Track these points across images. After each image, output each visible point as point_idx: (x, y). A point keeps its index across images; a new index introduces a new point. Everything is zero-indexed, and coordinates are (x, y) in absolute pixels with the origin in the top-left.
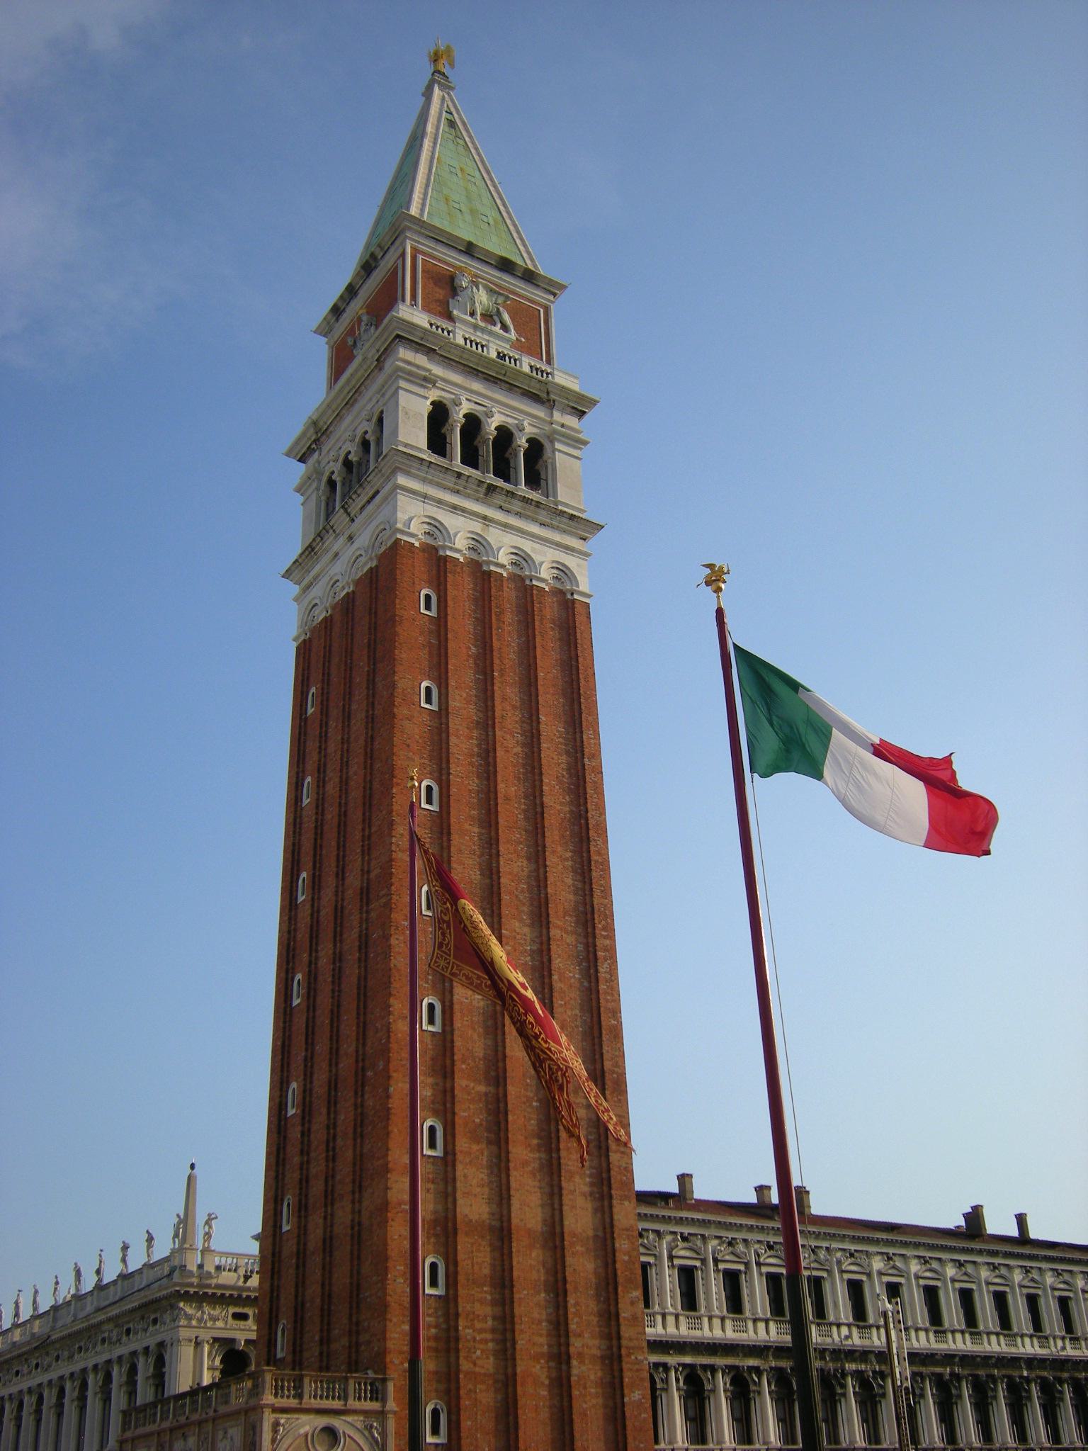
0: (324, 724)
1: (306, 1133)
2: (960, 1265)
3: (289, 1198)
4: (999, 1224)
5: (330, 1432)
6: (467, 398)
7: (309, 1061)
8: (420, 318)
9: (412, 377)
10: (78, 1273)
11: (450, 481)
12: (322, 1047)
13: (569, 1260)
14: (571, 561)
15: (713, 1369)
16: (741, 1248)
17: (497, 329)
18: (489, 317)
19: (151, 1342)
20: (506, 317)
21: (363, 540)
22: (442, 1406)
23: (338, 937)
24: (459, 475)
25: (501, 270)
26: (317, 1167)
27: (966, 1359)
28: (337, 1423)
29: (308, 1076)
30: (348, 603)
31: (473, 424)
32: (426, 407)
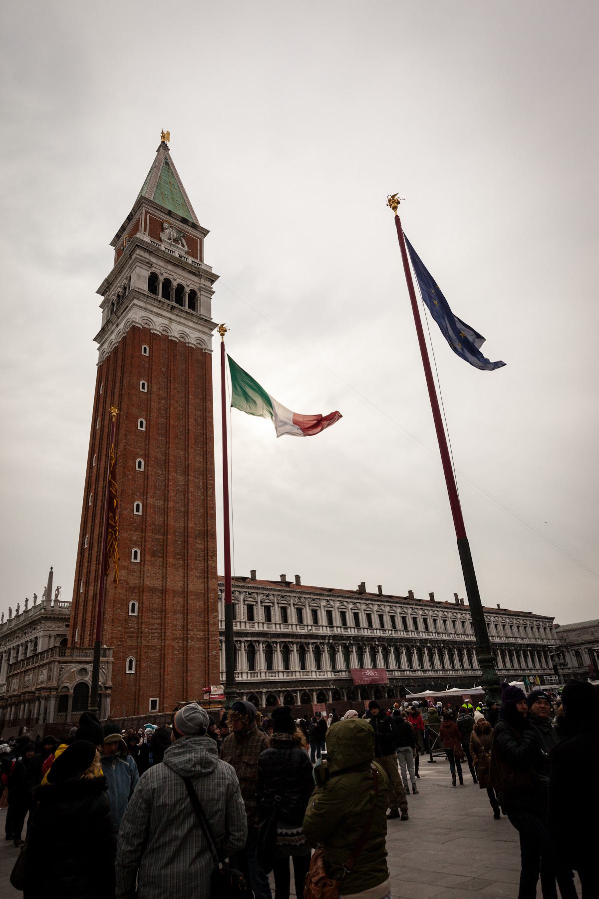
0: (105, 397)
1: (90, 554)
2: (354, 604)
4: (371, 589)
5: (85, 670)
6: (165, 272)
7: (93, 527)
8: (147, 239)
9: (142, 262)
10: (10, 610)
11: (156, 304)
15: (259, 642)
16: (272, 597)
17: (180, 246)
19: (32, 637)
20: (184, 241)
22: (134, 659)
24: (160, 301)
27: (355, 638)
29: (92, 532)
30: (115, 351)
31: (167, 282)
32: (147, 274)
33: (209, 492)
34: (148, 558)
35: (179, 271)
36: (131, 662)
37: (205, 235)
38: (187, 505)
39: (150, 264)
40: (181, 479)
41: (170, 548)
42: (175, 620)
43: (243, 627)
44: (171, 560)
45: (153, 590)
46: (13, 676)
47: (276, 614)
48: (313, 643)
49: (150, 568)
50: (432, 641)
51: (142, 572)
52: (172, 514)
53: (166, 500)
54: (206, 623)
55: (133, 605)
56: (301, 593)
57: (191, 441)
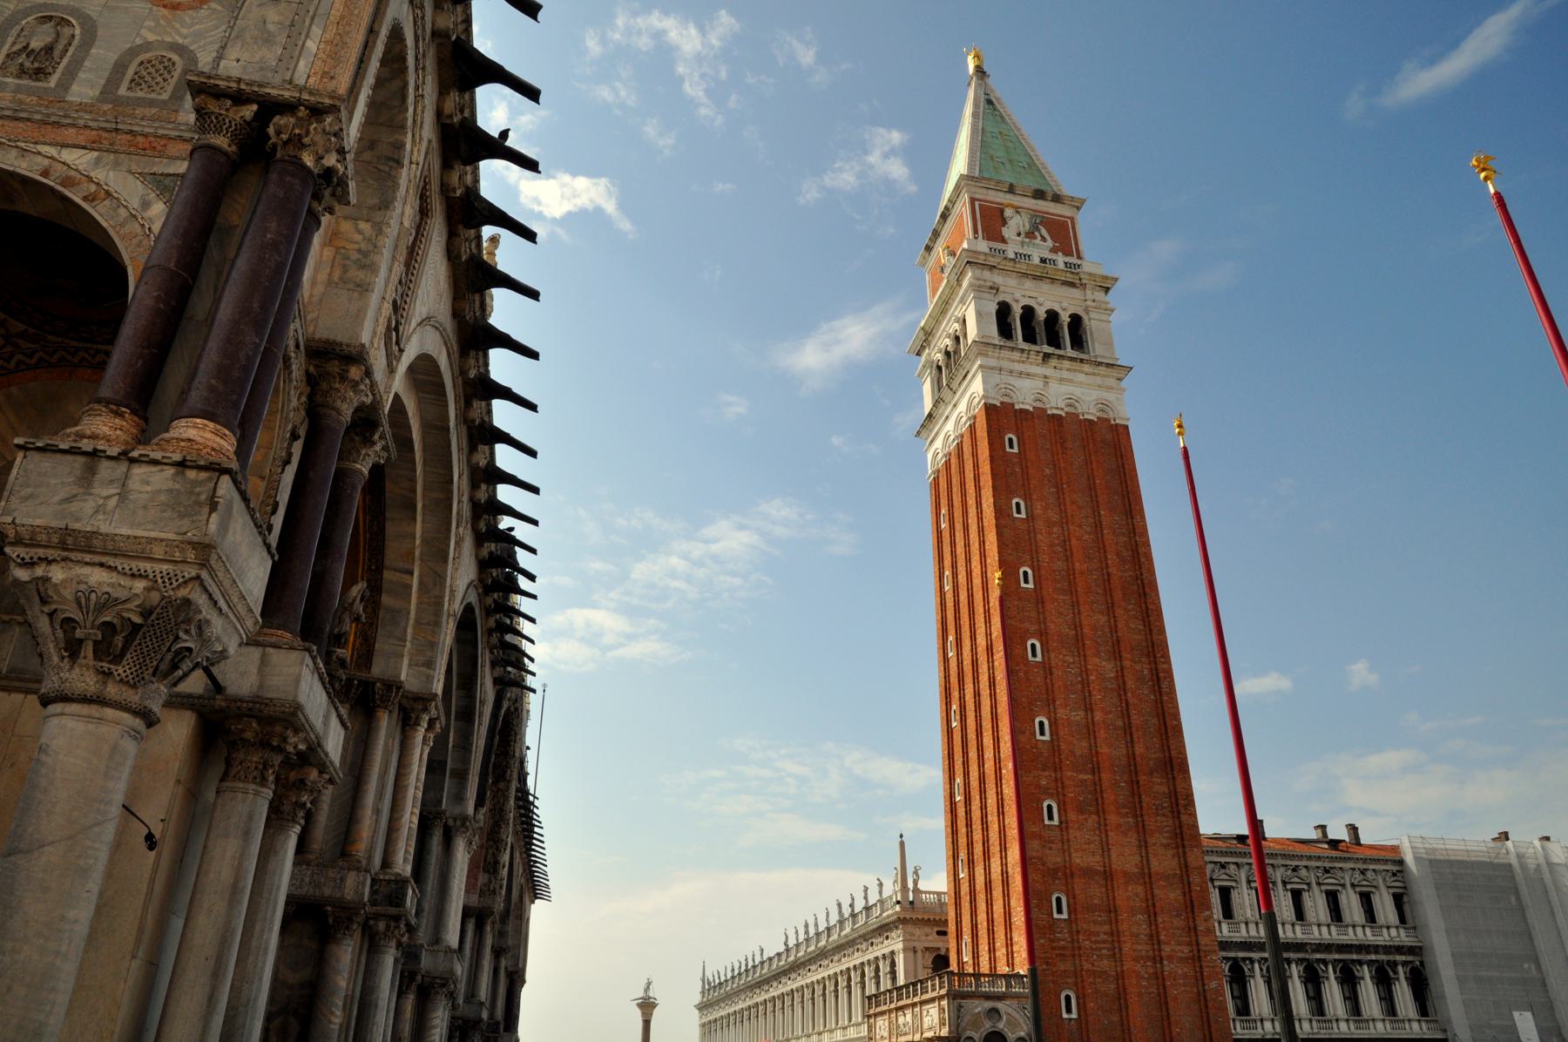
1: (968, 813)
3: (963, 855)
7: (966, 764)
10: (839, 905)
11: (1016, 355)
12: (973, 754)
13: (1156, 891)
14: (1111, 397)
16: (1303, 872)
17: (1038, 241)
18: (1030, 235)
19: (886, 951)
21: (962, 407)
23: (976, 680)
24: (1022, 351)
25: (1034, 197)
26: (978, 836)
28: (999, 1005)
31: (1028, 312)
32: (993, 308)
33: (1164, 685)
34: (1072, 816)
35: (1045, 287)
36: (1068, 998)
37: (1078, 208)
38: (1126, 714)
39: (995, 289)
40: (1109, 668)
41: (1109, 797)
42: (1134, 925)
43: (1253, 933)
44: (1113, 819)
45: (1088, 872)
46: (876, 1015)
47: (1316, 905)
48: (1405, 964)
49: (1078, 834)
51: (1065, 841)
52: (1102, 734)
53: (1089, 709)
54: (1192, 930)
55: (1059, 900)
56: (1365, 861)
57: (1118, 594)
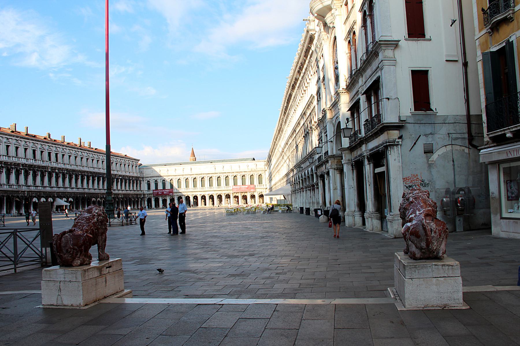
27: (6, 163)
50: (59, 169)
